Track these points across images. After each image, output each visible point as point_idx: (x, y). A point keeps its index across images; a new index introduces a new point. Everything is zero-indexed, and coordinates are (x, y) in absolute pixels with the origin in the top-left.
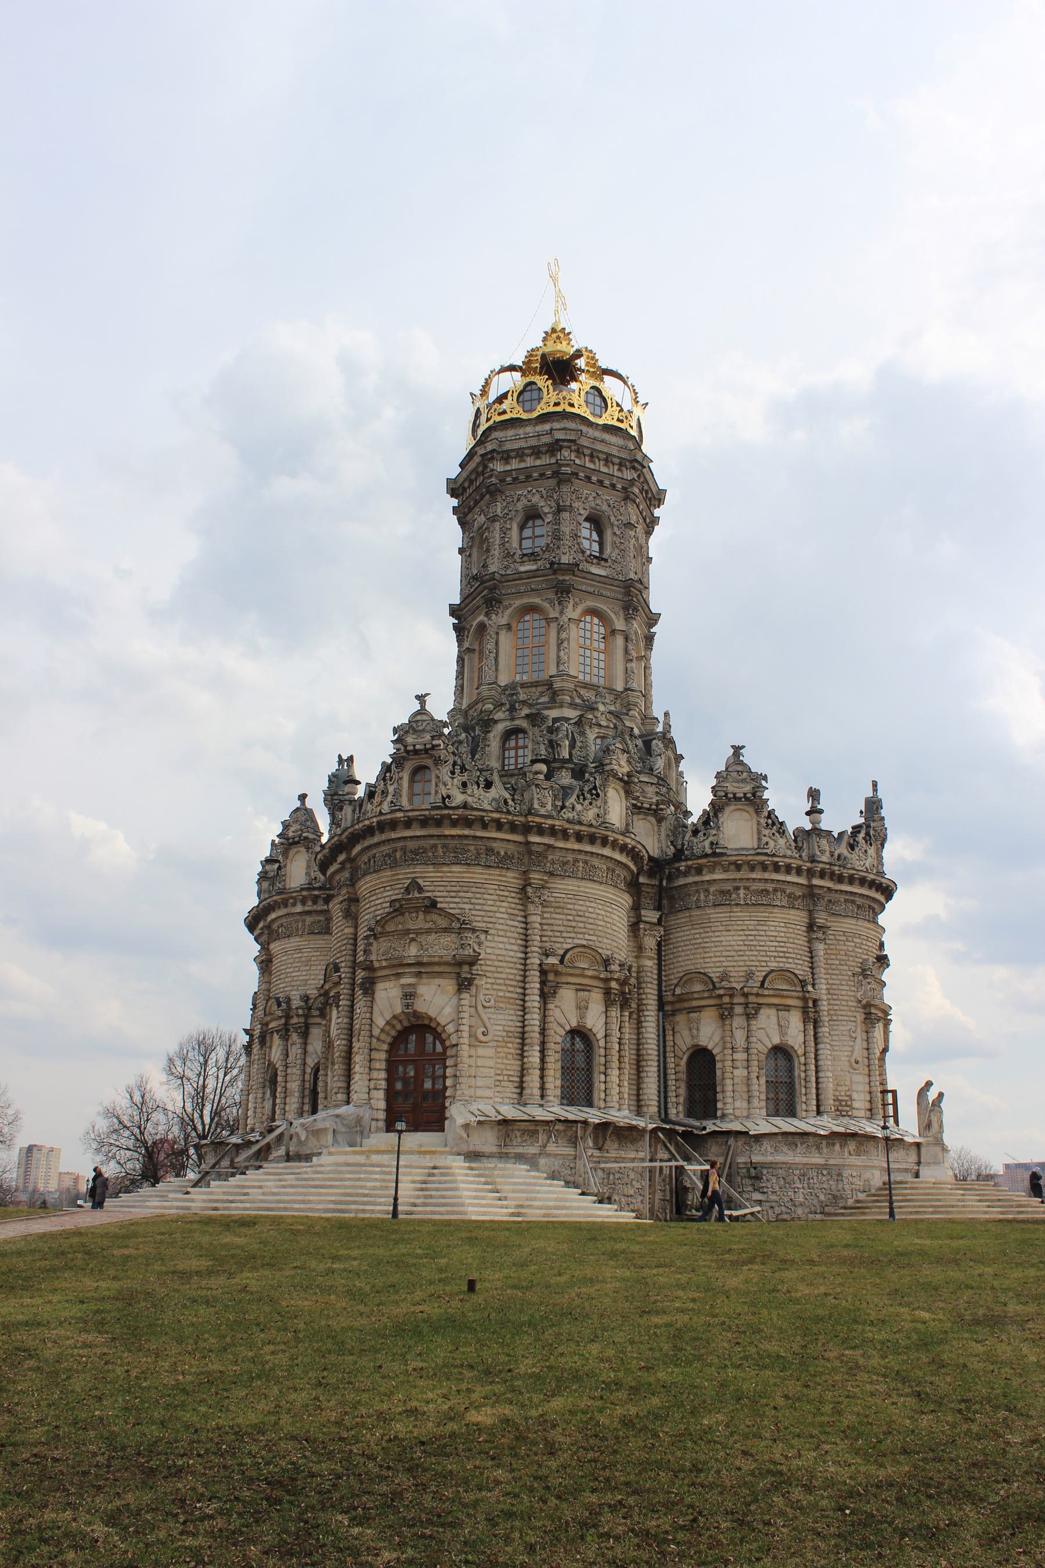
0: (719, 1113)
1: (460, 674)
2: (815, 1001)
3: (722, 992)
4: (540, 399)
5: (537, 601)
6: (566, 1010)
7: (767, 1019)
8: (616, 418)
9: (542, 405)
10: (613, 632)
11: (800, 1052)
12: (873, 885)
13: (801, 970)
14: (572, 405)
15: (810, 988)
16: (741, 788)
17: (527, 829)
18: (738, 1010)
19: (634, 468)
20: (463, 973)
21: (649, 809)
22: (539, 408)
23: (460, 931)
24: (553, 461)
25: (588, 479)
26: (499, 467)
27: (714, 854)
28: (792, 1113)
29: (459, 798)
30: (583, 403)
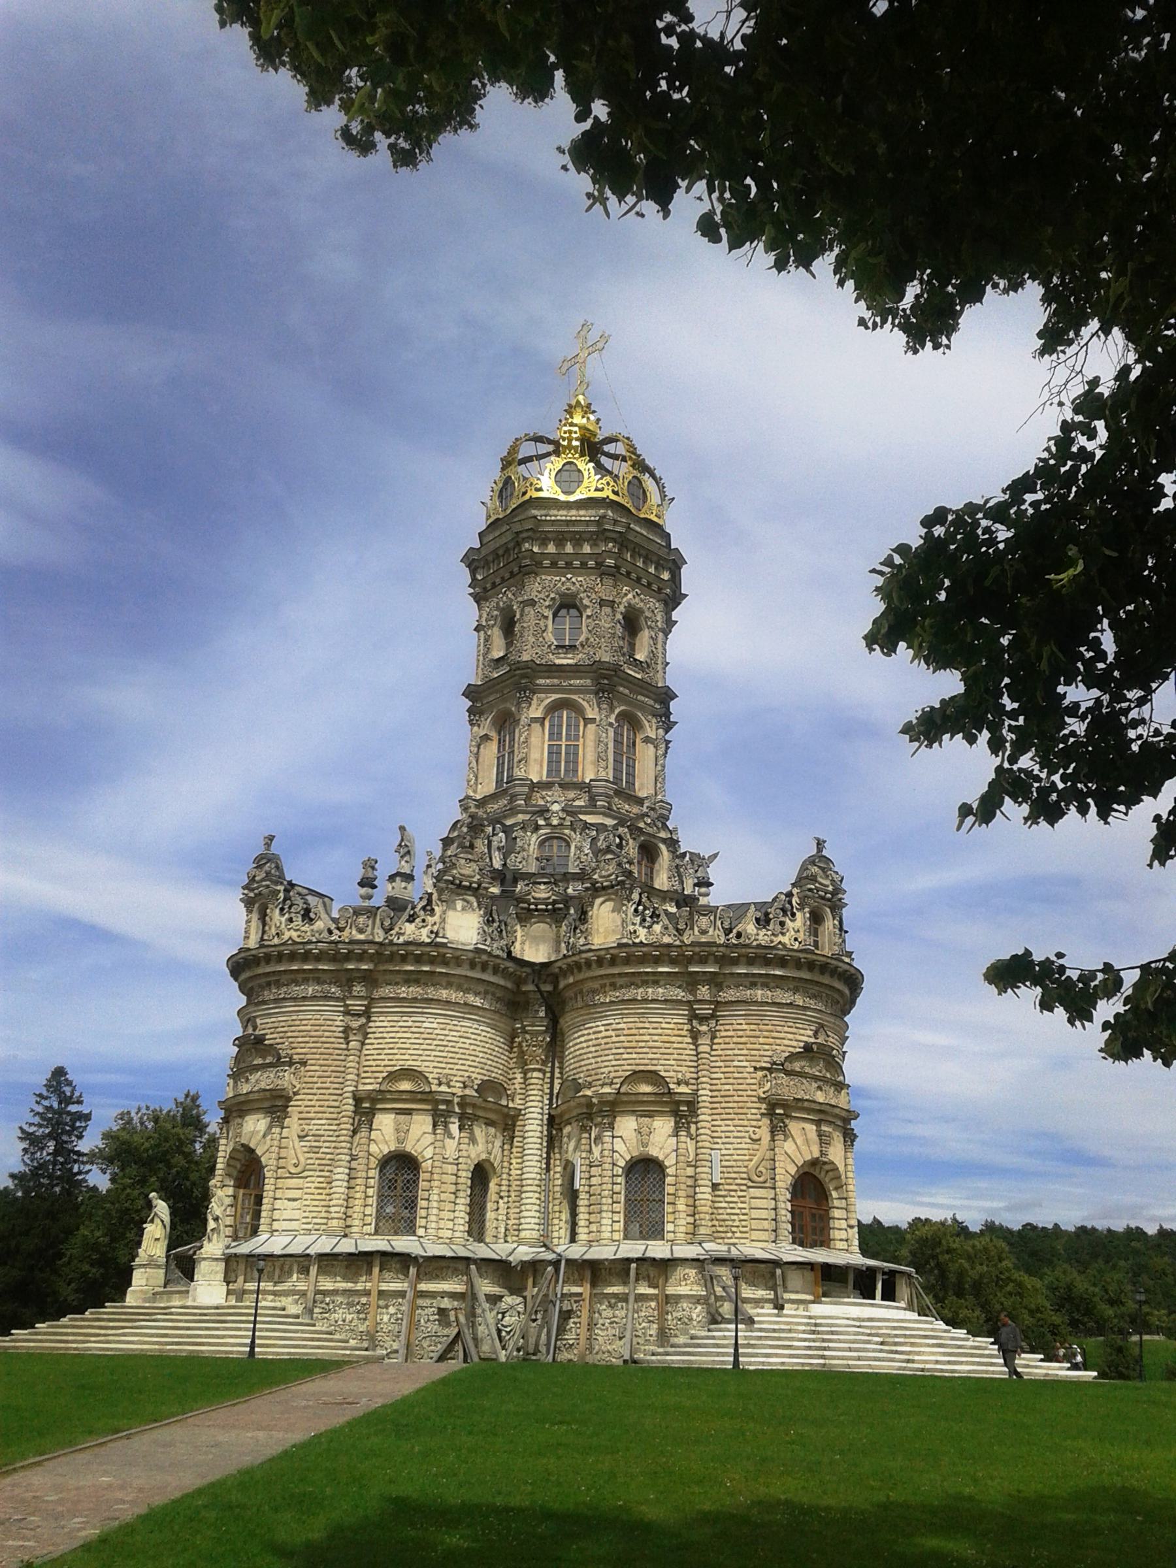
6: (386, 1133)
7: (627, 1125)
8: (593, 489)
9: (514, 501)
13: (675, 1067)
14: (540, 490)
15: (683, 1089)
21: (547, 910)
25: (554, 564)
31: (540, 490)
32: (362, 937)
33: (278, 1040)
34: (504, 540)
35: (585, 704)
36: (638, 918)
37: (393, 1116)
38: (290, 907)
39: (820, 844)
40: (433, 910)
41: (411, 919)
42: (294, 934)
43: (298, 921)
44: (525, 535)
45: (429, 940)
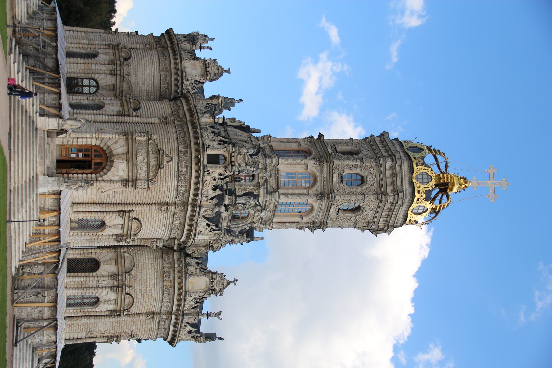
0: (69, 274)
1: (289, 141)
2: (120, 315)
3: (124, 276)
4: (423, 183)
5: (318, 184)
7: (112, 296)
9: (419, 184)
10: (302, 217)
11: (97, 309)
12: (174, 336)
15: (125, 313)
16: (217, 284)
17: (194, 206)
18: (116, 283)
19: (385, 226)
20: (129, 181)
22: (417, 182)
23: (148, 180)
24: (389, 191)
26: (388, 165)
27: (186, 273)
28: (68, 305)
29: (208, 178)
30: (419, 205)
31: (418, 200)
32: (202, 211)
33: (159, 177)
34: (399, 184)
35: (310, 217)
36: (197, 297)
37: (121, 223)
38: (222, 179)
39: (220, 338)
40: (210, 231)
41: (208, 225)
42: (208, 182)
43: (214, 183)
44: (396, 198)
45: (197, 230)
